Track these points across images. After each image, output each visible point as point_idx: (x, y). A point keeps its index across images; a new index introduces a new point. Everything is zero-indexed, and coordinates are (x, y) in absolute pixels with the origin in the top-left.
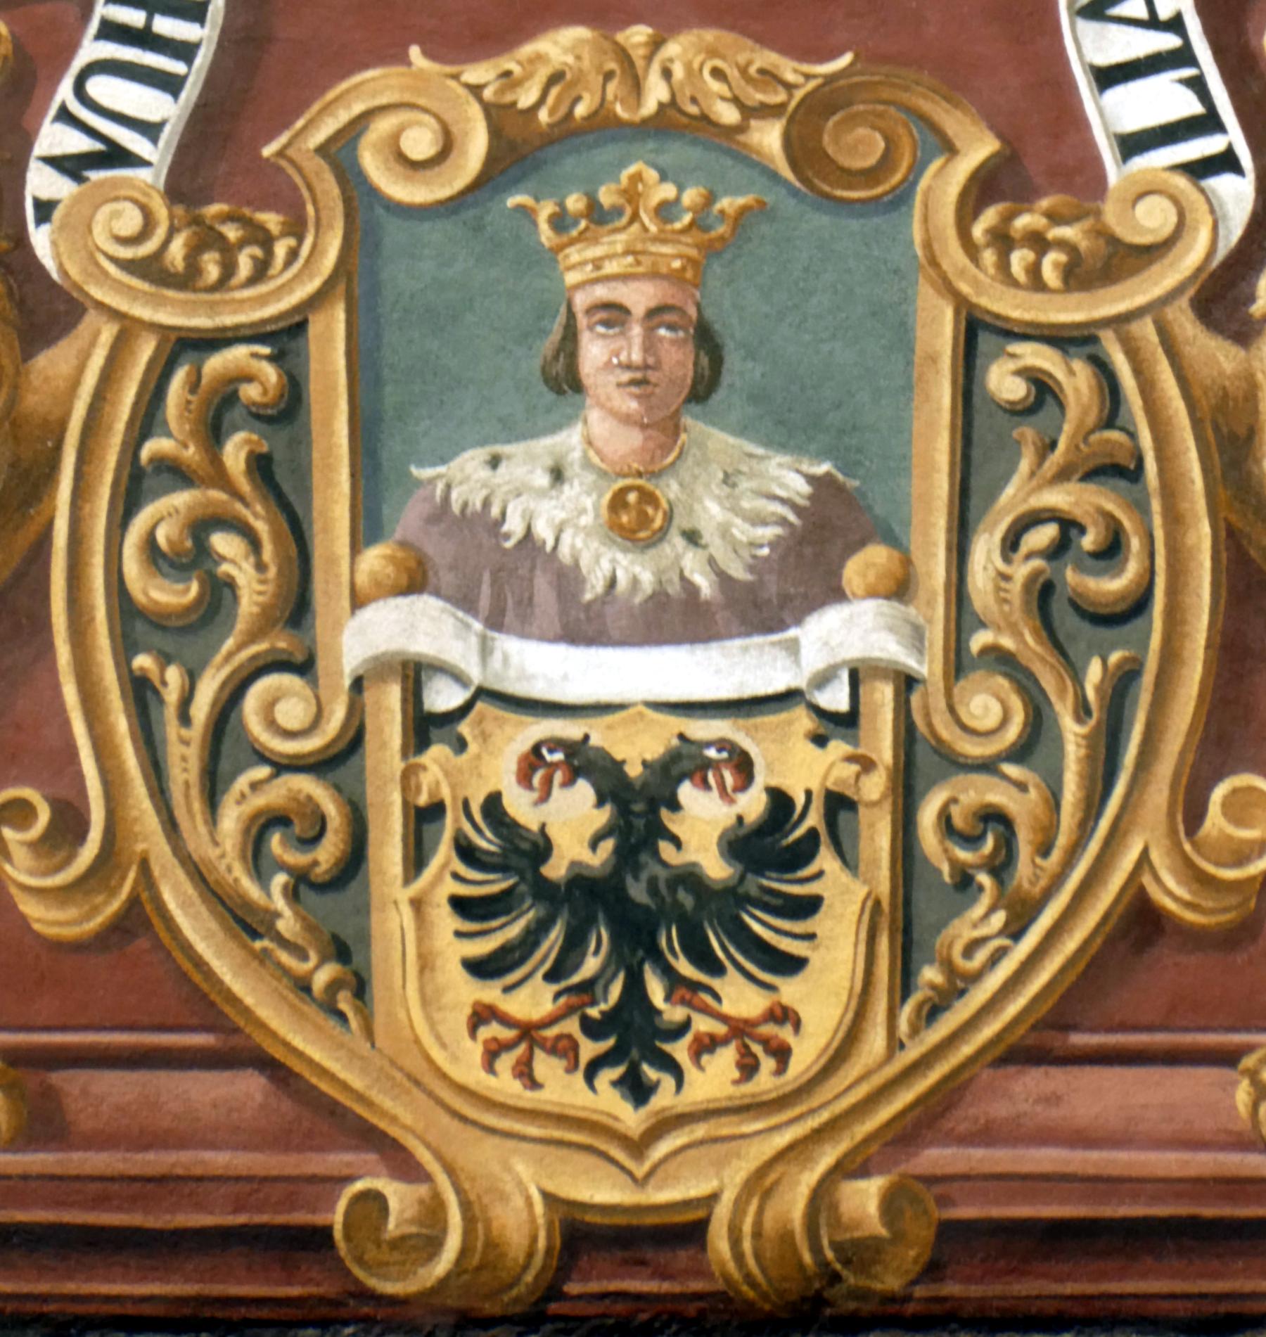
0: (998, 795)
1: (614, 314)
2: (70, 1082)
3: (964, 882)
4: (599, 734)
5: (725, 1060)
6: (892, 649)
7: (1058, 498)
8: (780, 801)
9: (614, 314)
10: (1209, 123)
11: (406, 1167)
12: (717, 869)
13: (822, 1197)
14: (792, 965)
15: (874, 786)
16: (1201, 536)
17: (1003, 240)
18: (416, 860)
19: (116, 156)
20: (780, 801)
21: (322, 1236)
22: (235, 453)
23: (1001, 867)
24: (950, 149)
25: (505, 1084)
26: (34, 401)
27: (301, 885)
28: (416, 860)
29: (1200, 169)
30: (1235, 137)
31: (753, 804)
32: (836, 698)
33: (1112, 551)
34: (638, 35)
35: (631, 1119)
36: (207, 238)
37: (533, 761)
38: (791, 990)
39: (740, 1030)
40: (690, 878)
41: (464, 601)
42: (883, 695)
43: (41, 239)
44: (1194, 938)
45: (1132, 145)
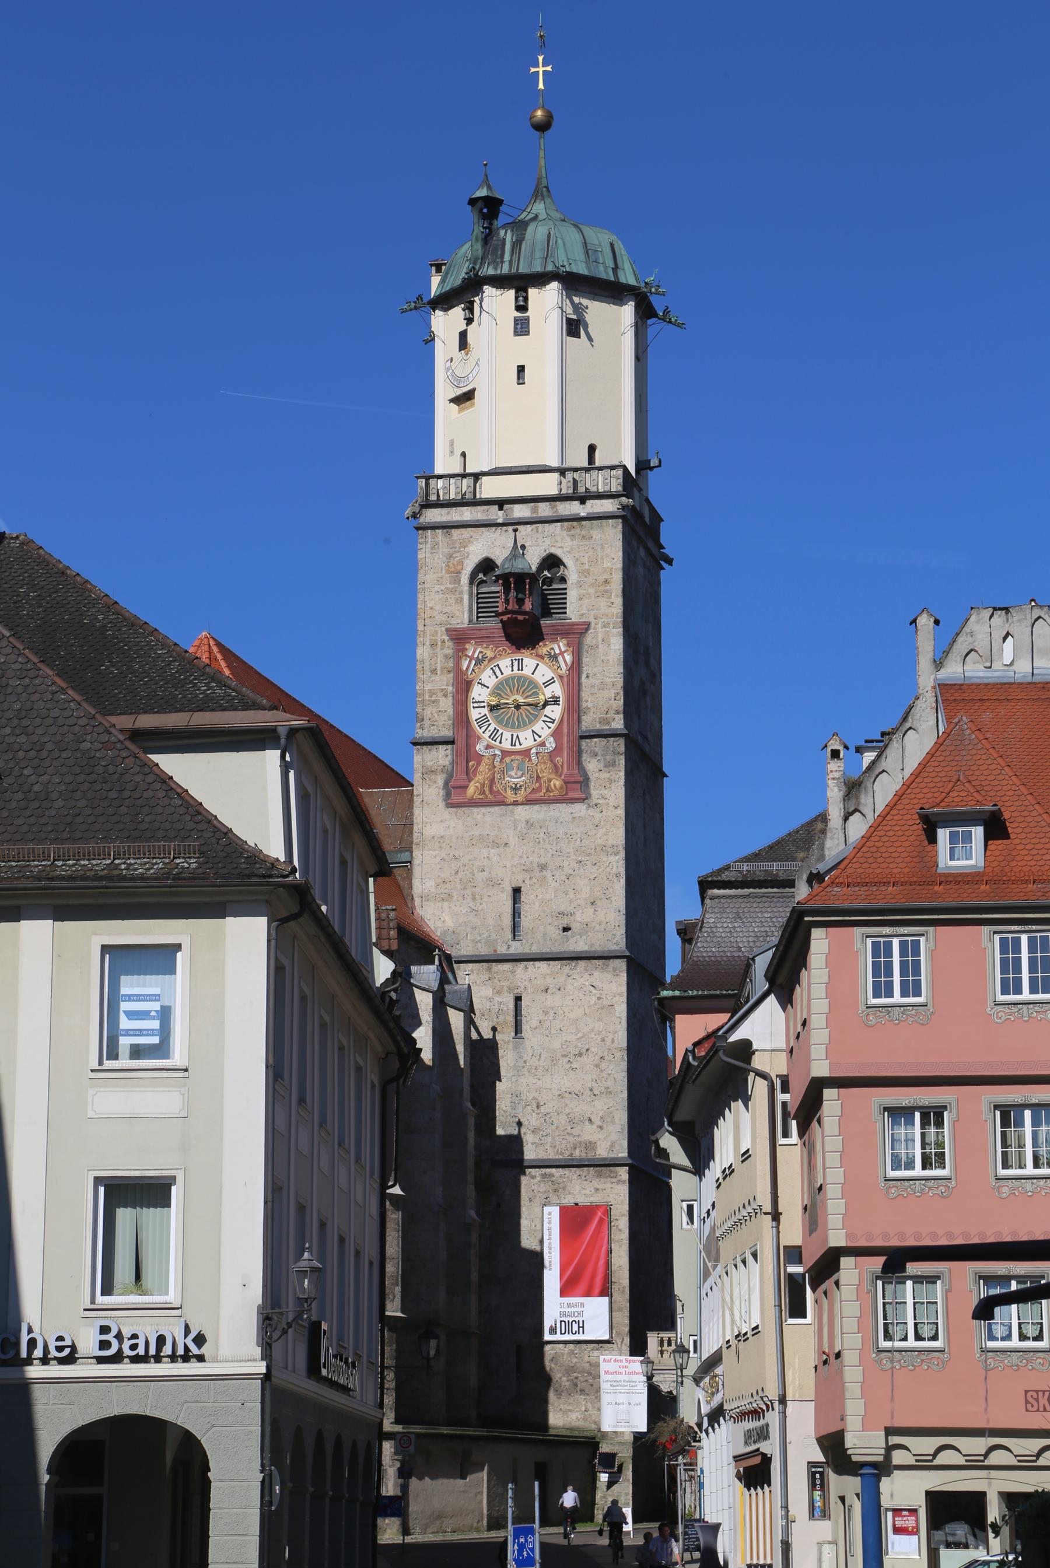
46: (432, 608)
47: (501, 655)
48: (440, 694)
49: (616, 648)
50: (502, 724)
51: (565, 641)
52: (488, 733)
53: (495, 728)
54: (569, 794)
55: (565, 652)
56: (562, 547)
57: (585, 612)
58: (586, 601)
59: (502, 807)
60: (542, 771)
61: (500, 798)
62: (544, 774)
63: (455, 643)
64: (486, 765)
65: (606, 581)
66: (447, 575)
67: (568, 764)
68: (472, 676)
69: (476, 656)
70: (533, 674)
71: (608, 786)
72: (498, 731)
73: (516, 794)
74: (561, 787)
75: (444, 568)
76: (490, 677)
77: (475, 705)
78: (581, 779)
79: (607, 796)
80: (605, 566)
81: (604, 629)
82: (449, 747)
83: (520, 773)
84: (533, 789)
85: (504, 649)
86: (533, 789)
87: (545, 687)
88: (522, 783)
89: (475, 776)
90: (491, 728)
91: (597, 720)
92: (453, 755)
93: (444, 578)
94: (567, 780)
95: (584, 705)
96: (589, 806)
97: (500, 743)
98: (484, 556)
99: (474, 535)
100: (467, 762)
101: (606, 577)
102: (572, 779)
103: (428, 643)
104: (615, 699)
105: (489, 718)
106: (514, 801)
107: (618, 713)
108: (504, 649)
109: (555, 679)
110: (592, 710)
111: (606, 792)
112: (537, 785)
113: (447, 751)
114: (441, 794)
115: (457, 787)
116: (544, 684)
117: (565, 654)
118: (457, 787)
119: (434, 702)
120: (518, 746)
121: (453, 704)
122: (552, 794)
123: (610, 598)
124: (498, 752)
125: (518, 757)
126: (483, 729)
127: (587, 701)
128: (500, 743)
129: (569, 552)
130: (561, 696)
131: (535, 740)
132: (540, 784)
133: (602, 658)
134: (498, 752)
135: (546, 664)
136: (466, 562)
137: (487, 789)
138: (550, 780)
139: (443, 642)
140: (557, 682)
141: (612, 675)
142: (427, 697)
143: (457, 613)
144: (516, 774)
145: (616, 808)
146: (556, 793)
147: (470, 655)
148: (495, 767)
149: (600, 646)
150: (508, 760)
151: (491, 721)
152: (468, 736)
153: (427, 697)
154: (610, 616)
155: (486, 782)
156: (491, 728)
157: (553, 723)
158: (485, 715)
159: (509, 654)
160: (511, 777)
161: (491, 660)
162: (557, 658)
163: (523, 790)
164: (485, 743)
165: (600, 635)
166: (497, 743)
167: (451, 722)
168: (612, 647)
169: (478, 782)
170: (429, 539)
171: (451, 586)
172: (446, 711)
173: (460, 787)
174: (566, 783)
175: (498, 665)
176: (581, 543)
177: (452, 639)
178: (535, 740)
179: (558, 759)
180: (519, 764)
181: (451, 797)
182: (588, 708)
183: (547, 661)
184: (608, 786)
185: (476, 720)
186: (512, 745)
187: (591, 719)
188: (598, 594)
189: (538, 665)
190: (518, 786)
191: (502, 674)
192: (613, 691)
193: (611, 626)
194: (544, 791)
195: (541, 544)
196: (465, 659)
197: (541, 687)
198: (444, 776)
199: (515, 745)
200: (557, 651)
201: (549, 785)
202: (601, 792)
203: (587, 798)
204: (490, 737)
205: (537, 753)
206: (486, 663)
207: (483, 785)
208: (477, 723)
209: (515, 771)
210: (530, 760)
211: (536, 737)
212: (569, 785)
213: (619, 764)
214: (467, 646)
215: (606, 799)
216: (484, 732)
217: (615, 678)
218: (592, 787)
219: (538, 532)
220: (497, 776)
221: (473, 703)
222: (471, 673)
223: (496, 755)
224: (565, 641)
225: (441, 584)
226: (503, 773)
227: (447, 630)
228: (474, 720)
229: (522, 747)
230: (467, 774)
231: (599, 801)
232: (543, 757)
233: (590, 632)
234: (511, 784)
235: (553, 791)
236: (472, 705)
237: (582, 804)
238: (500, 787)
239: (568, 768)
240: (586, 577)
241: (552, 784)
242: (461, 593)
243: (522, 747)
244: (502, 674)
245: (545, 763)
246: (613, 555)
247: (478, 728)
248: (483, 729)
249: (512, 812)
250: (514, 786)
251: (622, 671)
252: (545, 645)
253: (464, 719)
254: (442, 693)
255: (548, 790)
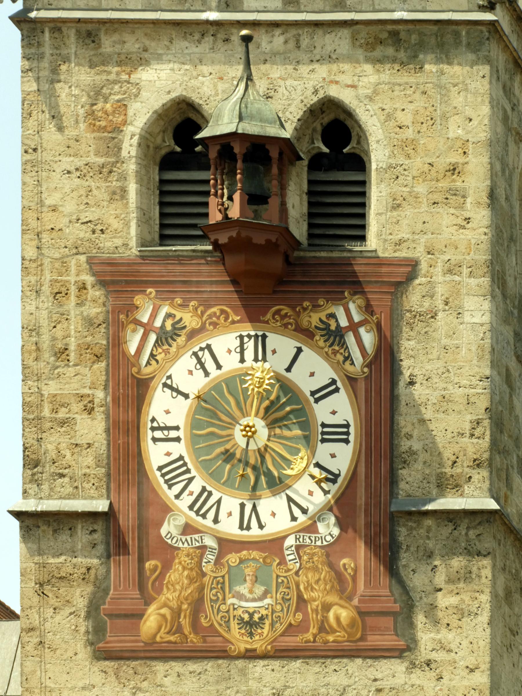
0: (279, 614)
1: (249, 575)
2: (207, 638)
3: (277, 622)
4: (248, 610)
5: (258, 636)
6: (271, 602)
7: (284, 590)
8: (262, 615)
9: (249, 575)
10: (296, 559)
11: (233, 644)
12: (257, 620)
13: (266, 647)
14: (263, 628)
15: (270, 614)
16: (295, 593)
17: (280, 569)
18: (234, 620)
19: (209, 562)
20: (262, 615)
21: (226, 651)
22: (219, 586)
23: (280, 620)
24: (275, 561)
25: (241, 638)
26: (204, 582)
27: (225, 622)
28: (234, 620)
29: (295, 563)
30: (298, 560)
31: (260, 615)
32: (267, 607)
33: (288, 594)
34: (251, 551)
35: (251, 641)
36: (217, 569)
37: (243, 612)
38: (263, 630)
39: (259, 634)
40: (255, 621)
41: (237, 598)
42: (270, 606)
43: (204, 569)
44: (295, 626)
45: (290, 561)
46: (54, 209)
47: (215, 325)
48: (76, 407)
49: (476, 320)
50: (218, 481)
51: (360, 301)
52: (187, 500)
53: (204, 489)
54: (369, 638)
55: (361, 324)
56: (354, 86)
57: (406, 236)
58: (408, 211)
59: (220, 662)
60: (309, 587)
61: (216, 642)
62: (314, 594)
63: (108, 292)
64: (184, 568)
65: (454, 170)
66: (88, 135)
67: (368, 574)
68: (149, 369)
69: (158, 323)
70: (288, 370)
71: (454, 623)
72: (210, 494)
73: (251, 635)
74: (352, 624)
75: (81, 119)
76: (191, 372)
77: (158, 434)
78: (397, 607)
79: (453, 646)
80: (451, 135)
81: (448, 278)
82: (99, 526)
83: (259, 590)
84: (290, 625)
85: (222, 312)
86: (290, 625)
87: (317, 401)
88: (264, 612)
89: (159, 591)
90: (196, 487)
91: (433, 479)
92: (108, 544)
93: (83, 140)
94: (365, 607)
95: (404, 445)
96: (413, 665)
97: (216, 521)
98: (173, 95)
99: (152, 45)
100: (141, 561)
101: (453, 160)
102: (377, 607)
103: (46, 289)
104: (472, 435)
105: (190, 466)
106: (247, 650)
107: (477, 464)
108: (222, 312)
109: (339, 384)
110: (422, 457)
111: (450, 636)
112: (299, 616)
113: (96, 536)
114: (83, 629)
115: (118, 616)
116: (313, 393)
117: (362, 330)
118: (118, 616)
119: (63, 423)
120: (255, 531)
121: (107, 431)
122: (331, 638)
123: (461, 207)
124: (210, 542)
125: (255, 554)
126: (177, 489)
127: (409, 437)
128: (216, 521)
129: (371, 99)
130: (352, 423)
131: (294, 519)
132: (306, 615)
133: (445, 341)
134: (210, 542)
135: (318, 349)
136: (134, 107)
137: (185, 622)
138: (327, 607)
139: (83, 287)
140: (342, 391)
141: (464, 382)
142: (46, 412)
143: (115, 224)
144: (251, 592)
145: (472, 671)
146: (341, 635)
147: (145, 320)
148: (204, 575)
149: (440, 315)
150: (233, 559)
151: (194, 473)
152: (141, 503)
153: (46, 412)
154: (462, 248)
155: (185, 606)
156: (196, 487)
157: (334, 481)
158: (181, 458)
159: (233, 322)
160: (240, 597)
161: (193, 334)
162: (342, 337)
163: (267, 627)
164: (181, 521)
165: (441, 290)
166: (208, 522)
167: (103, 470)
168: (467, 318)
169: (165, 605)
170: (47, 50)
171: (101, 160)
172: (89, 445)
173: (126, 616)
174: (362, 614)
175: (209, 347)
176: (398, 81)
177: (103, 283)
178: (294, 519)
179: (345, 561)
180: (257, 569)
181: (104, 635)
182: (412, 453)
183: (321, 343)
184: (454, 623)
185: (160, 468)
186: (241, 527)
187: (420, 476)
188: (437, 197)
189: (299, 350)
190: (256, 617)
191: (219, 367)
192: (469, 417)
193: (465, 271)
194: (313, 630)
195: (305, 75)
196: (134, 331)
197: (308, 401)
198: (89, 589)
199: (248, 528)
200: (344, 322)
201: (325, 619)
202: (439, 636)
203: (408, 649)
204: (191, 507)
205: (298, 548)
206: (181, 340)
207: (177, 613)
208: (163, 475)
209: (248, 584)
210: (283, 562)
211: (297, 512)
212: (370, 621)
213: (479, 577)
214: (138, 300)
215: (450, 651)
216: (177, 497)
217: (471, 387)
218: (420, 626)
219: (298, 47)
220: (208, 594)
221: (153, 429)
222: (148, 363)
223: (204, 548)
224: (360, 301)
225: (75, 155)
226: (223, 588)
227: (90, 261)
228: (155, 467)
229: (265, 531)
230: (142, 586)
231: (434, 656)
232: (311, 556)
233: (417, 281)
234: (240, 612)
235: (335, 631)
236: (150, 434)
237: (398, 661)
238: (216, 620)
239: (368, 583)
240: (408, 156)
241: (331, 615)
242: (123, 177)
243: (265, 531)
244: (219, 367)
245: (315, 569)
246: (469, 112)
247: (165, 487)
248: (177, 489)
249: (243, 672)
250: (246, 617)
251: (487, 372)
252: (316, 307)
253: (133, 465)
254: (81, 405)
255: (323, 628)
